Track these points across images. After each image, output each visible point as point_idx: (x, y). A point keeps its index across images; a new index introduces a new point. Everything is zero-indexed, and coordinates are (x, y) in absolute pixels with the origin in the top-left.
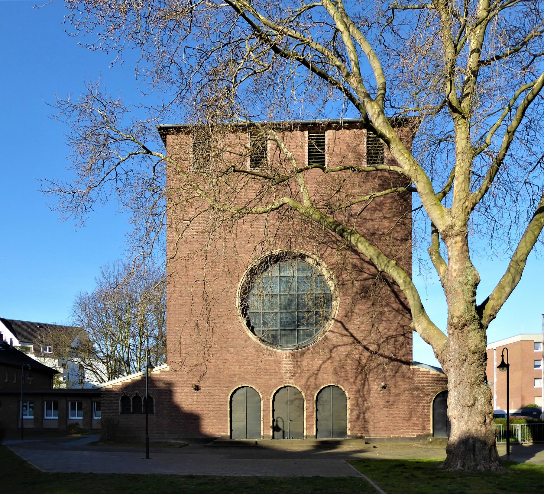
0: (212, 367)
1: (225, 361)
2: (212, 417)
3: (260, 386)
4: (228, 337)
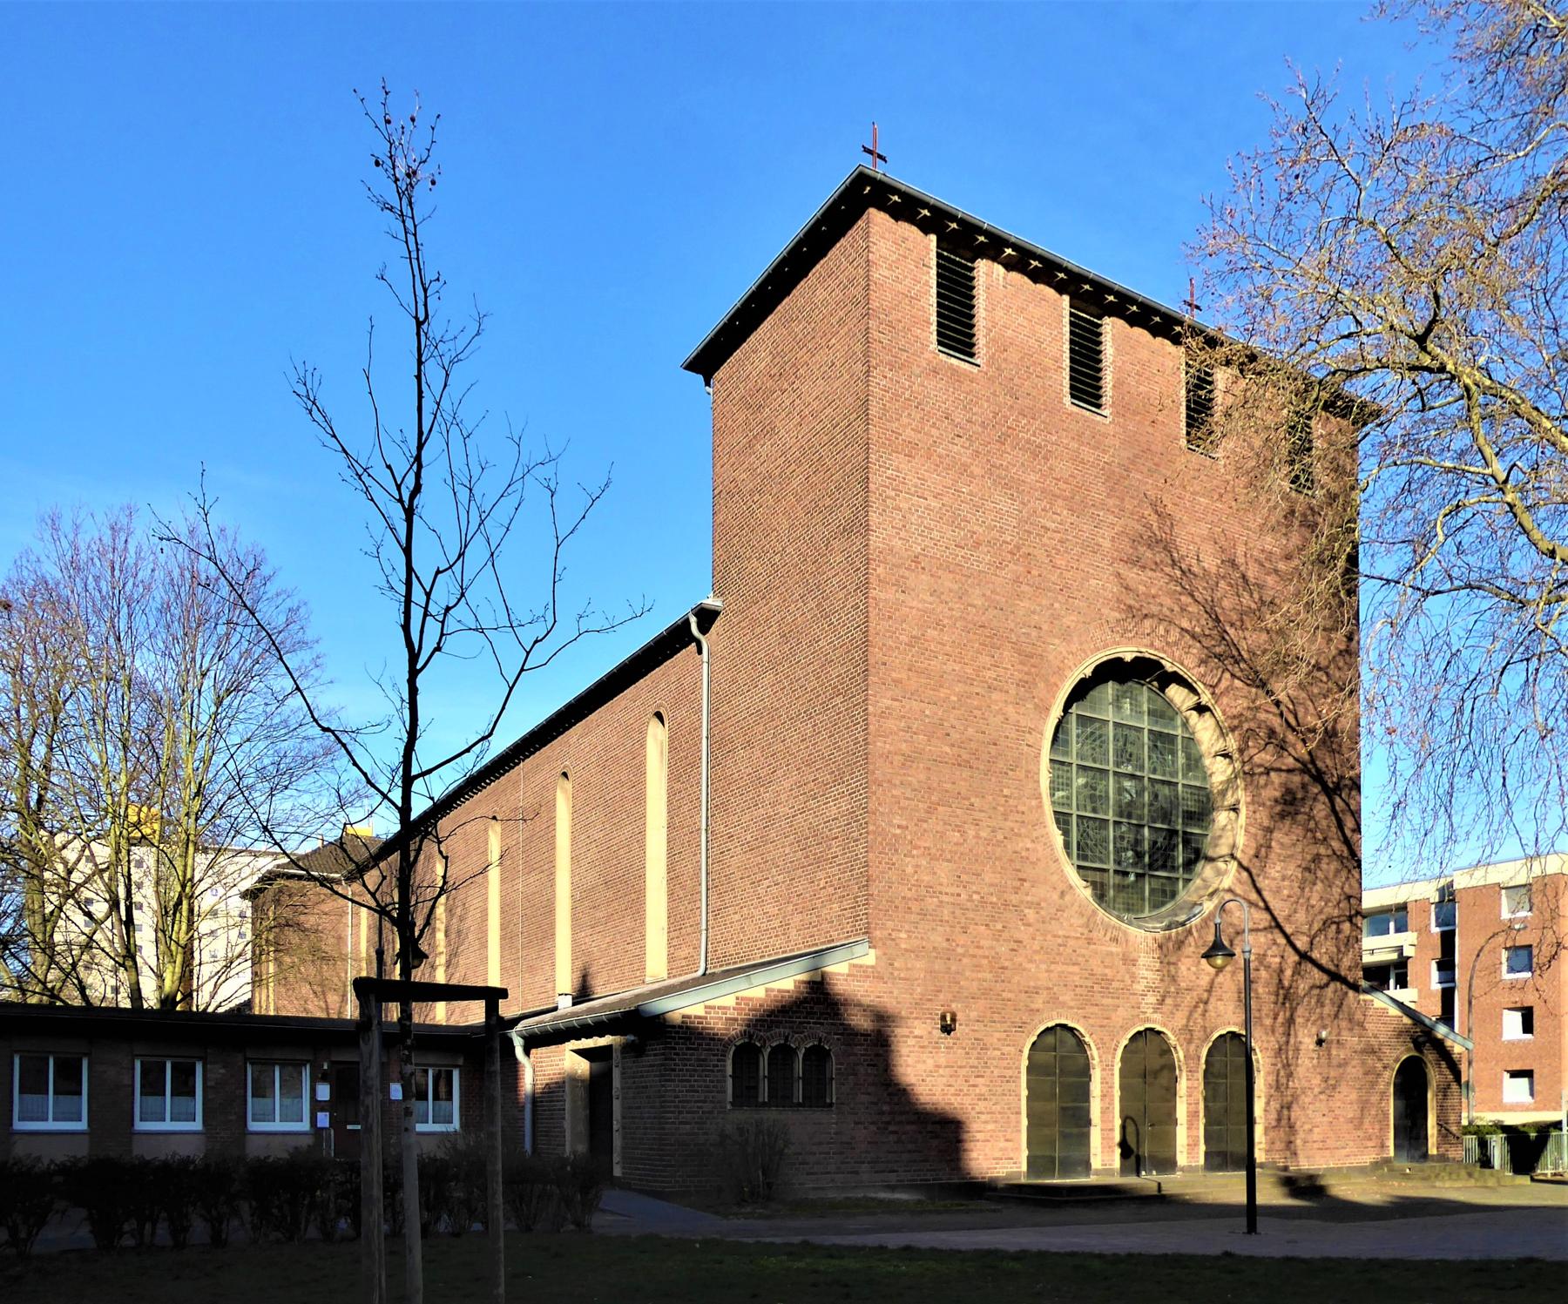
0: (985, 962)
1: (1015, 946)
2: (983, 1117)
3: (1093, 1026)
4: (1021, 875)
